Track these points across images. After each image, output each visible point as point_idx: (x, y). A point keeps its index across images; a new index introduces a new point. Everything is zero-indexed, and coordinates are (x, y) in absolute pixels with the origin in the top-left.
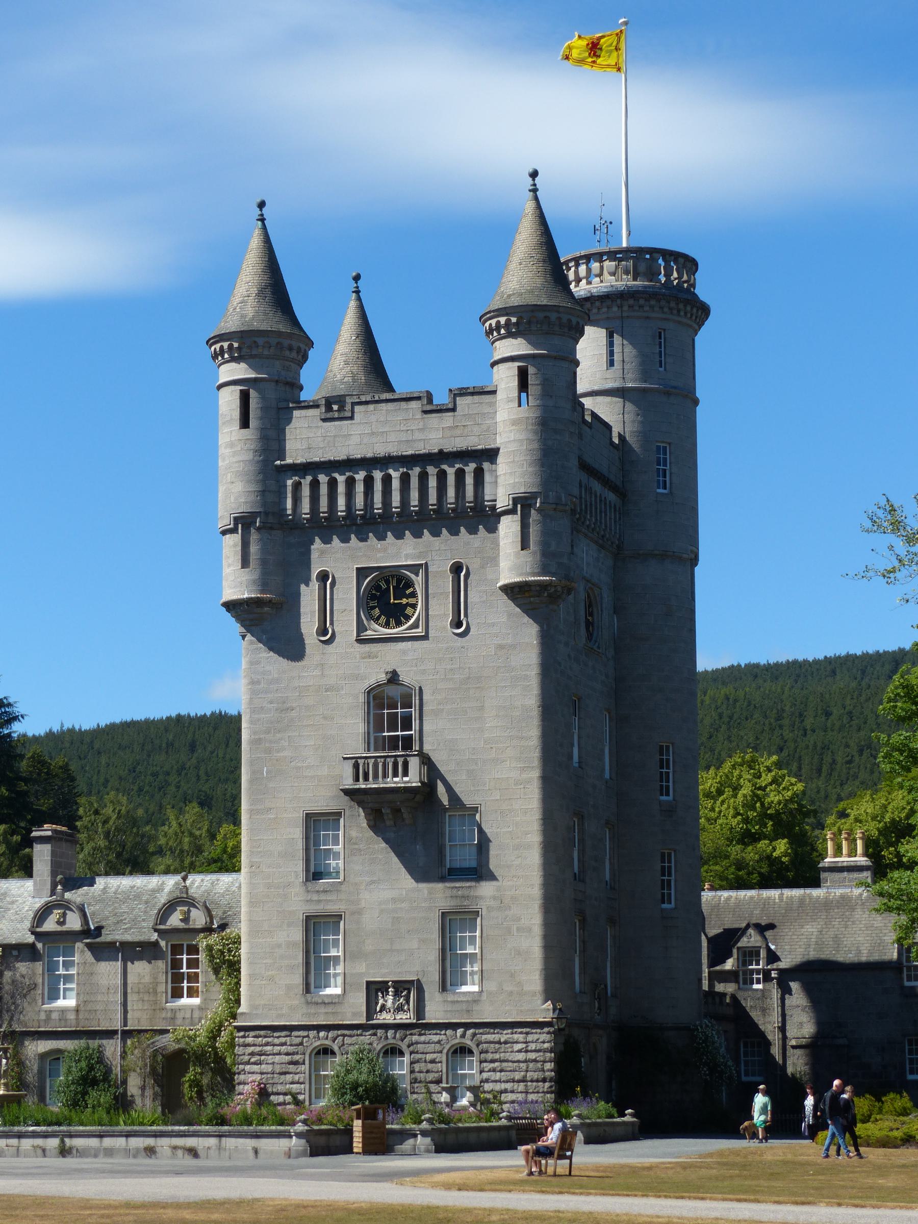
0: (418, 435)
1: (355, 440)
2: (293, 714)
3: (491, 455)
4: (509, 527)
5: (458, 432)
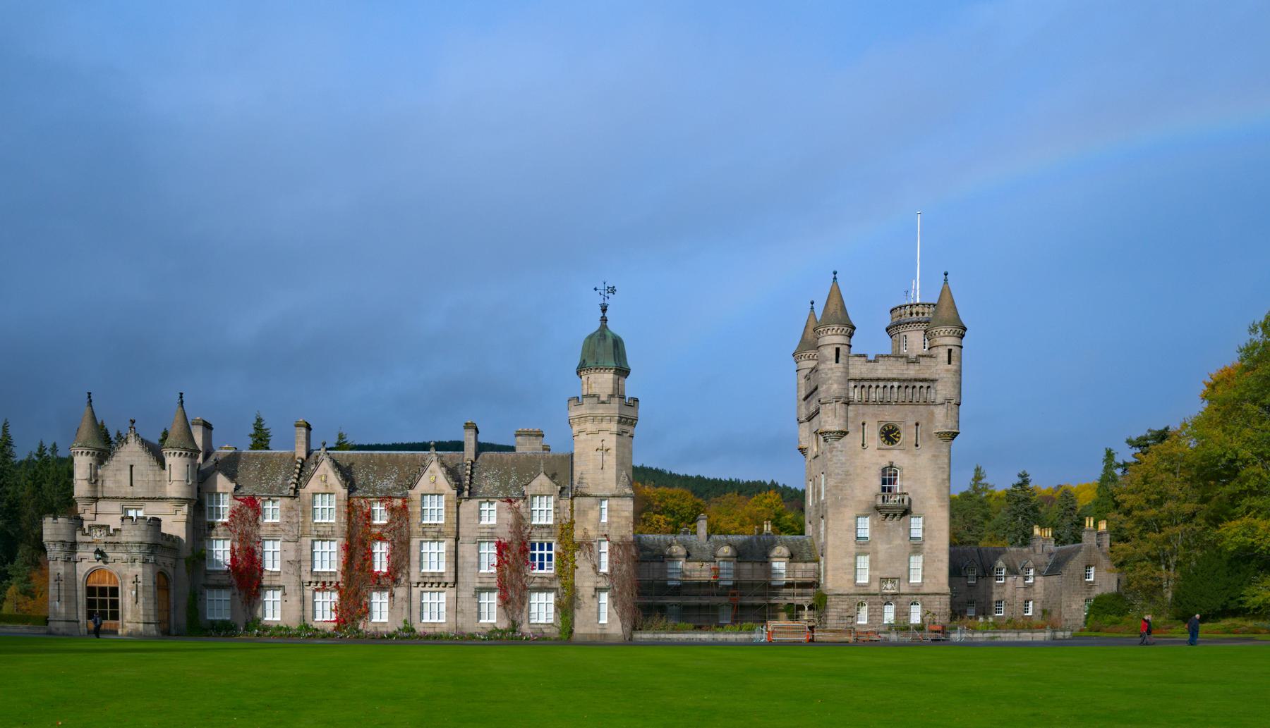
0: (905, 372)
1: (880, 371)
2: (851, 477)
3: (933, 381)
5: (920, 372)
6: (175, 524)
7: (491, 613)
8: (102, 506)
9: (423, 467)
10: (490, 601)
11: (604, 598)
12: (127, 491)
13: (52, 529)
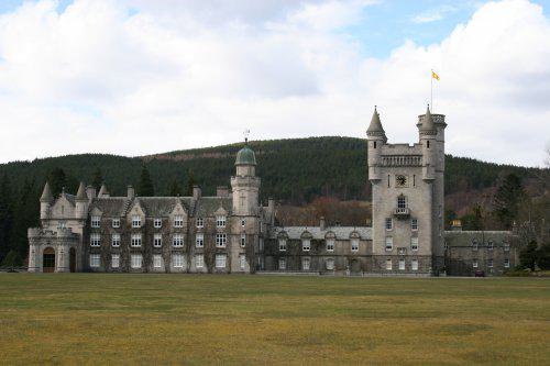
4: (424, 170)
6: (78, 229)
7: (199, 263)
8: (52, 222)
9: (174, 203)
10: (200, 259)
11: (243, 257)
12: (60, 216)
13: (31, 233)
